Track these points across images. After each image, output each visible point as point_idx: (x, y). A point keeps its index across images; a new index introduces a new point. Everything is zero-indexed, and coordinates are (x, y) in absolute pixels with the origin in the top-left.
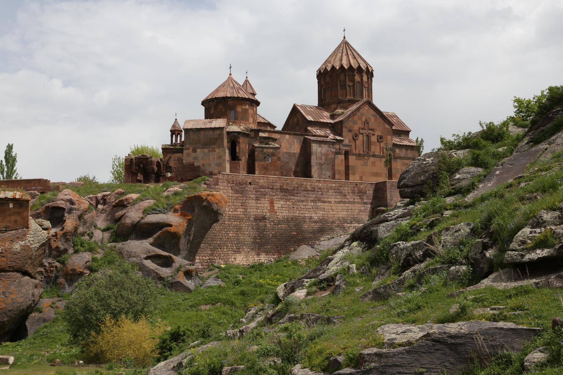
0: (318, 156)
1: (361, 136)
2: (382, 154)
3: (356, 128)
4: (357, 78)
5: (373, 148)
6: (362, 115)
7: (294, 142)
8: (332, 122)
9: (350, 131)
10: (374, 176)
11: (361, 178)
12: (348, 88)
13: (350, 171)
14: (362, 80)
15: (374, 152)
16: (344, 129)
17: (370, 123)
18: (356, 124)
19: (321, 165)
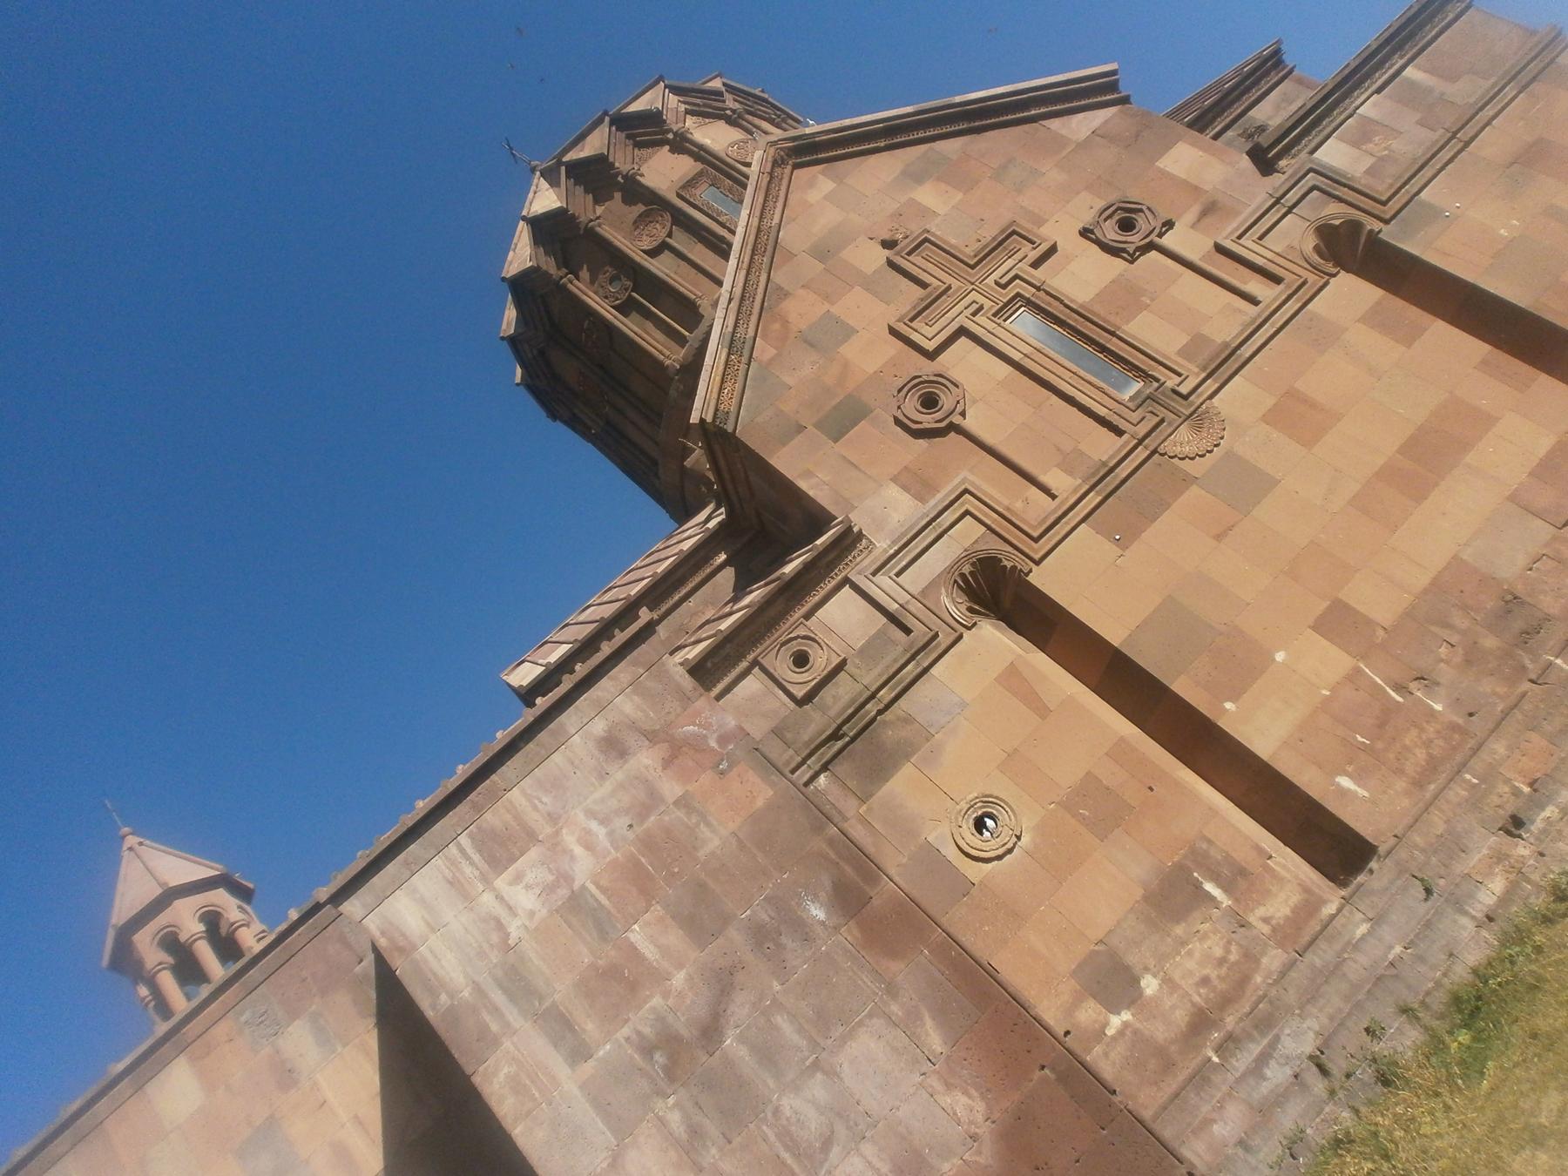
0: (561, 990)
1: (963, 362)
2: (1255, 285)
3: (871, 356)
4: (663, 171)
5: (1151, 331)
6: (824, 252)
7: (286, 1076)
8: (710, 518)
9: (842, 419)
10: (1417, 489)
11: (1338, 622)
12: (662, 267)
13: (1182, 687)
14: (701, 154)
15: (1198, 340)
16: (785, 461)
17: (938, 230)
18: (848, 332)
19: (682, 1055)
